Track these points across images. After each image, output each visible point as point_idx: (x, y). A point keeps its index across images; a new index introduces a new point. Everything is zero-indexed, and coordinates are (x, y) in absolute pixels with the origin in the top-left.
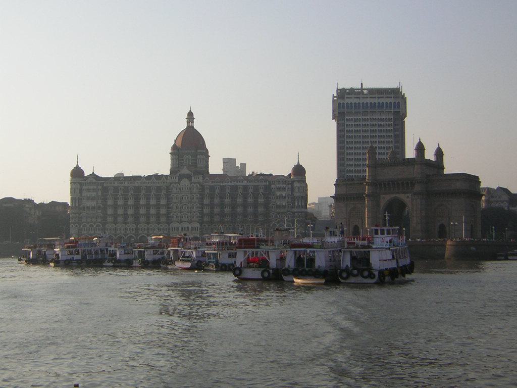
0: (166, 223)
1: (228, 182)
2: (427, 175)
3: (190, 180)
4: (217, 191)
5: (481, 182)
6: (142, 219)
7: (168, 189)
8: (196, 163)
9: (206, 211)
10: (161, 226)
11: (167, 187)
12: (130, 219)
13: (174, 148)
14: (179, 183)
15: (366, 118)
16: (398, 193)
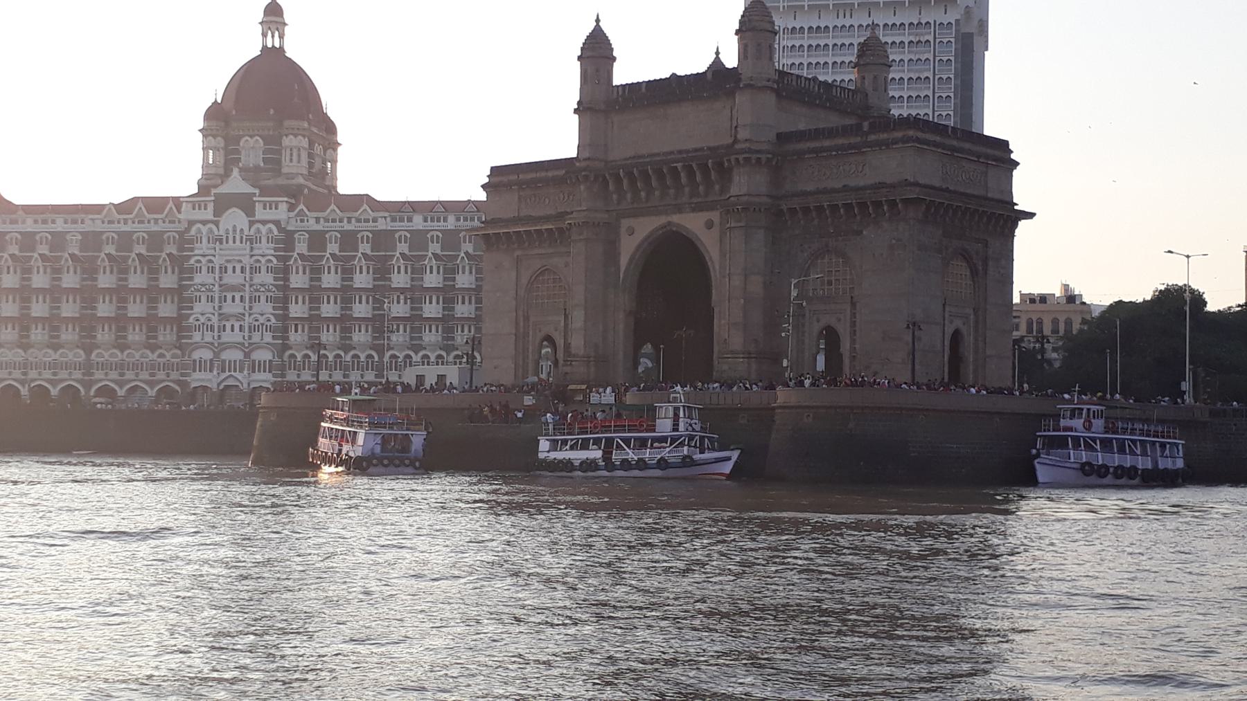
0: (176, 347)
1: (367, 221)
2: (779, 136)
3: (249, 211)
4: (333, 248)
5: (1016, 164)
6: (104, 336)
7: (185, 241)
8: (279, 162)
9: (297, 310)
10: (161, 356)
11: (181, 234)
12: (69, 335)
13: (215, 114)
14: (217, 224)
15: (848, 23)
16: (679, 209)
